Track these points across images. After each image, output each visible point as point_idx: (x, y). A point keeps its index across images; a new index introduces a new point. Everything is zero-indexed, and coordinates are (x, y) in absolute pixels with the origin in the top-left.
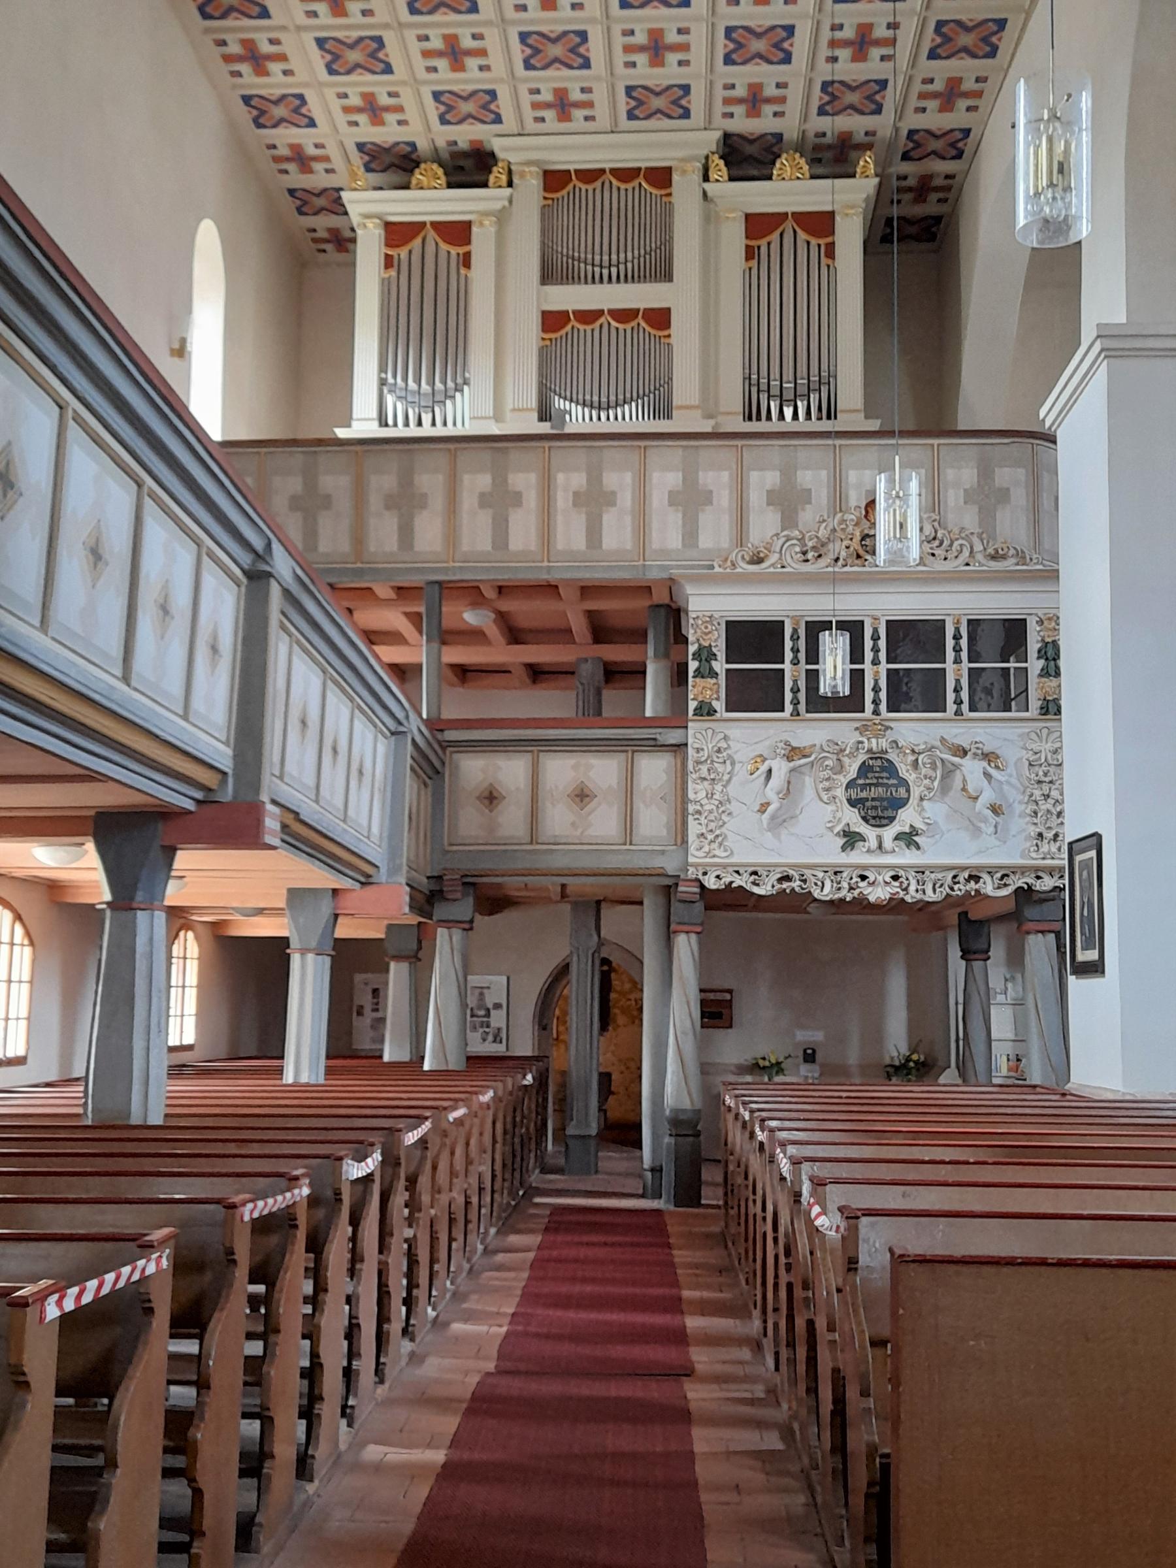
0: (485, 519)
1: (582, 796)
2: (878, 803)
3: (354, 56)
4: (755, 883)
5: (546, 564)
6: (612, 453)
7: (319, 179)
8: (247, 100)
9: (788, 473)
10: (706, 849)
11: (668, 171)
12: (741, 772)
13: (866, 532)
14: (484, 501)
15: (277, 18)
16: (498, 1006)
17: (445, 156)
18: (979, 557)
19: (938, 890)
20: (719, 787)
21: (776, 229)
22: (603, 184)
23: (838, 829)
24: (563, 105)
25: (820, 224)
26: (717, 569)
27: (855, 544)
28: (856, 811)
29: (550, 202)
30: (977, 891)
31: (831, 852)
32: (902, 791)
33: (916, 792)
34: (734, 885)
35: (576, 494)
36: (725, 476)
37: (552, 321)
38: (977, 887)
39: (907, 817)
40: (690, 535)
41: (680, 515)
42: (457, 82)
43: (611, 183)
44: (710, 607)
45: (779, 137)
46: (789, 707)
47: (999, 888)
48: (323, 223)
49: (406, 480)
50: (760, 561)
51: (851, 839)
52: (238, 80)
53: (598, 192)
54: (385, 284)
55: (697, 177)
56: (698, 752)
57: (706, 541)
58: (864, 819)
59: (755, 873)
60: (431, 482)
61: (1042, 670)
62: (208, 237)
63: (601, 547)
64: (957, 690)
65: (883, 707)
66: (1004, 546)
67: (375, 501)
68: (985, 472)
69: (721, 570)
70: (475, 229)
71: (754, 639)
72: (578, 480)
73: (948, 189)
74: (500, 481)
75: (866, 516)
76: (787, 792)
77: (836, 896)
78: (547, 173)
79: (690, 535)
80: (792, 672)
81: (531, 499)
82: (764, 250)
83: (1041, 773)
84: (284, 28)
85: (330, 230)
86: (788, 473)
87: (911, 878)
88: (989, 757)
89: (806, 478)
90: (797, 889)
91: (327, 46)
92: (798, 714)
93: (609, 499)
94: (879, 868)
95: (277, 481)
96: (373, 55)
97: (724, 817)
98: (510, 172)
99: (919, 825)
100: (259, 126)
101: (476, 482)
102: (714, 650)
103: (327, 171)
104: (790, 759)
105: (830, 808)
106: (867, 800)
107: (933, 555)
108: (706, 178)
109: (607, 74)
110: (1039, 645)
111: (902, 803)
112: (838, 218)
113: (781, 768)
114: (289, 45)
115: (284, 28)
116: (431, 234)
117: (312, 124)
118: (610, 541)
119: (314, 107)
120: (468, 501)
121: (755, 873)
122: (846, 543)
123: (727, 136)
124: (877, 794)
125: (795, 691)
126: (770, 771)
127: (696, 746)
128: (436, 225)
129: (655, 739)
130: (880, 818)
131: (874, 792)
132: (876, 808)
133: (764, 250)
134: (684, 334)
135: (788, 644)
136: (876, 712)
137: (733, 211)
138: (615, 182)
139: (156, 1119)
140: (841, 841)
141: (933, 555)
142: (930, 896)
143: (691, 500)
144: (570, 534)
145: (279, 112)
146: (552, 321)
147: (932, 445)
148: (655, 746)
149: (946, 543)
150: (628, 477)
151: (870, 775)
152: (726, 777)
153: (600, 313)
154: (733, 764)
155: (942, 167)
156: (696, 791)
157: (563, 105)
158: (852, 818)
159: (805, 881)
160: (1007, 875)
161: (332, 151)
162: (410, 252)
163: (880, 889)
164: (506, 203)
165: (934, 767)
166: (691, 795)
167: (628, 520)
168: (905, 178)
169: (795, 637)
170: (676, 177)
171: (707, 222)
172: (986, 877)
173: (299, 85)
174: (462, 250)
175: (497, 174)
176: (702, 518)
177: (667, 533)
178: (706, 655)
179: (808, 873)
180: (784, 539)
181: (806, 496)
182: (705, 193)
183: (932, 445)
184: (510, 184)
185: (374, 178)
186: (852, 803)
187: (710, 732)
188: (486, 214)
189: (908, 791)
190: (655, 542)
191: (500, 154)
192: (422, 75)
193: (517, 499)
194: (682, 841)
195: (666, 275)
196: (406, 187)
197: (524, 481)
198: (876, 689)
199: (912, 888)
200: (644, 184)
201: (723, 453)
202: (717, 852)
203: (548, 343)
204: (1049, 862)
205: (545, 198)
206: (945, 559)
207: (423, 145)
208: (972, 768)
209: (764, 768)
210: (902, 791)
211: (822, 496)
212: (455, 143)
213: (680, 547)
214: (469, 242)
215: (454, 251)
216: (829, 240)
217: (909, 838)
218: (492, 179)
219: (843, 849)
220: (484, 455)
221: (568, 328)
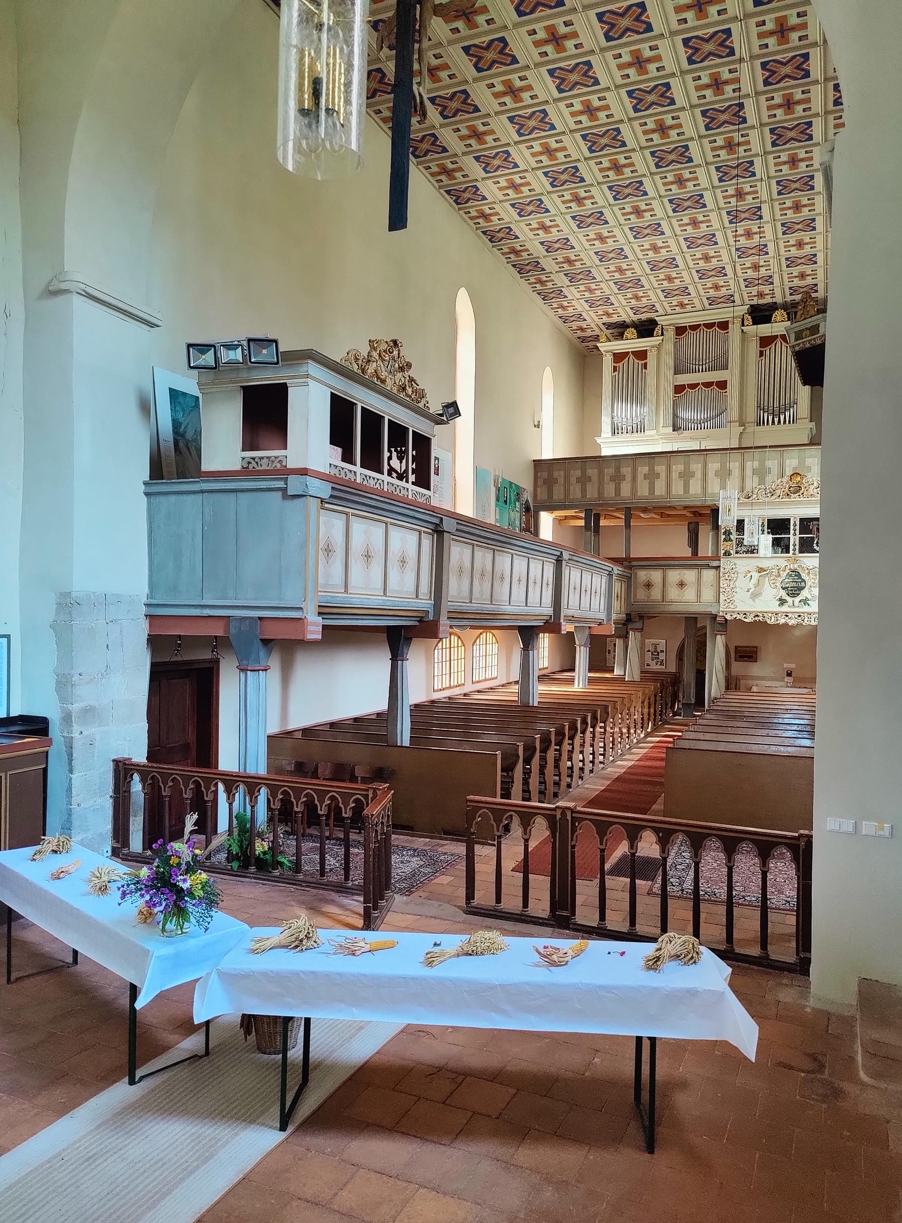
6: (694, 457)
7: (589, 333)
8: (560, 317)
9: (762, 462)
12: (741, 576)
14: (646, 477)
16: (662, 651)
24: (682, 305)
27: (787, 490)
31: (775, 606)
32: (803, 584)
33: (809, 584)
37: (679, 389)
45: (776, 303)
49: (618, 470)
54: (613, 378)
62: (548, 373)
67: (607, 478)
74: (652, 469)
78: (677, 328)
81: (663, 475)
82: (768, 352)
93: (692, 475)
99: (809, 597)
109: (699, 292)
113: (756, 575)
117: (585, 320)
120: (640, 477)
134: (733, 390)
139: (536, 704)
144: (678, 489)
146: (679, 389)
148: (708, 567)
153: (697, 385)
157: (682, 305)
158: (783, 594)
161: (593, 325)
175: (658, 330)
177: (714, 486)
178: (728, 533)
179: (765, 615)
186: (783, 589)
188: (653, 347)
190: (709, 491)
193: (658, 476)
197: (661, 469)
198: (795, 545)
201: (736, 455)
207: (628, 320)
209: (749, 575)
211: (775, 471)
220: (647, 460)
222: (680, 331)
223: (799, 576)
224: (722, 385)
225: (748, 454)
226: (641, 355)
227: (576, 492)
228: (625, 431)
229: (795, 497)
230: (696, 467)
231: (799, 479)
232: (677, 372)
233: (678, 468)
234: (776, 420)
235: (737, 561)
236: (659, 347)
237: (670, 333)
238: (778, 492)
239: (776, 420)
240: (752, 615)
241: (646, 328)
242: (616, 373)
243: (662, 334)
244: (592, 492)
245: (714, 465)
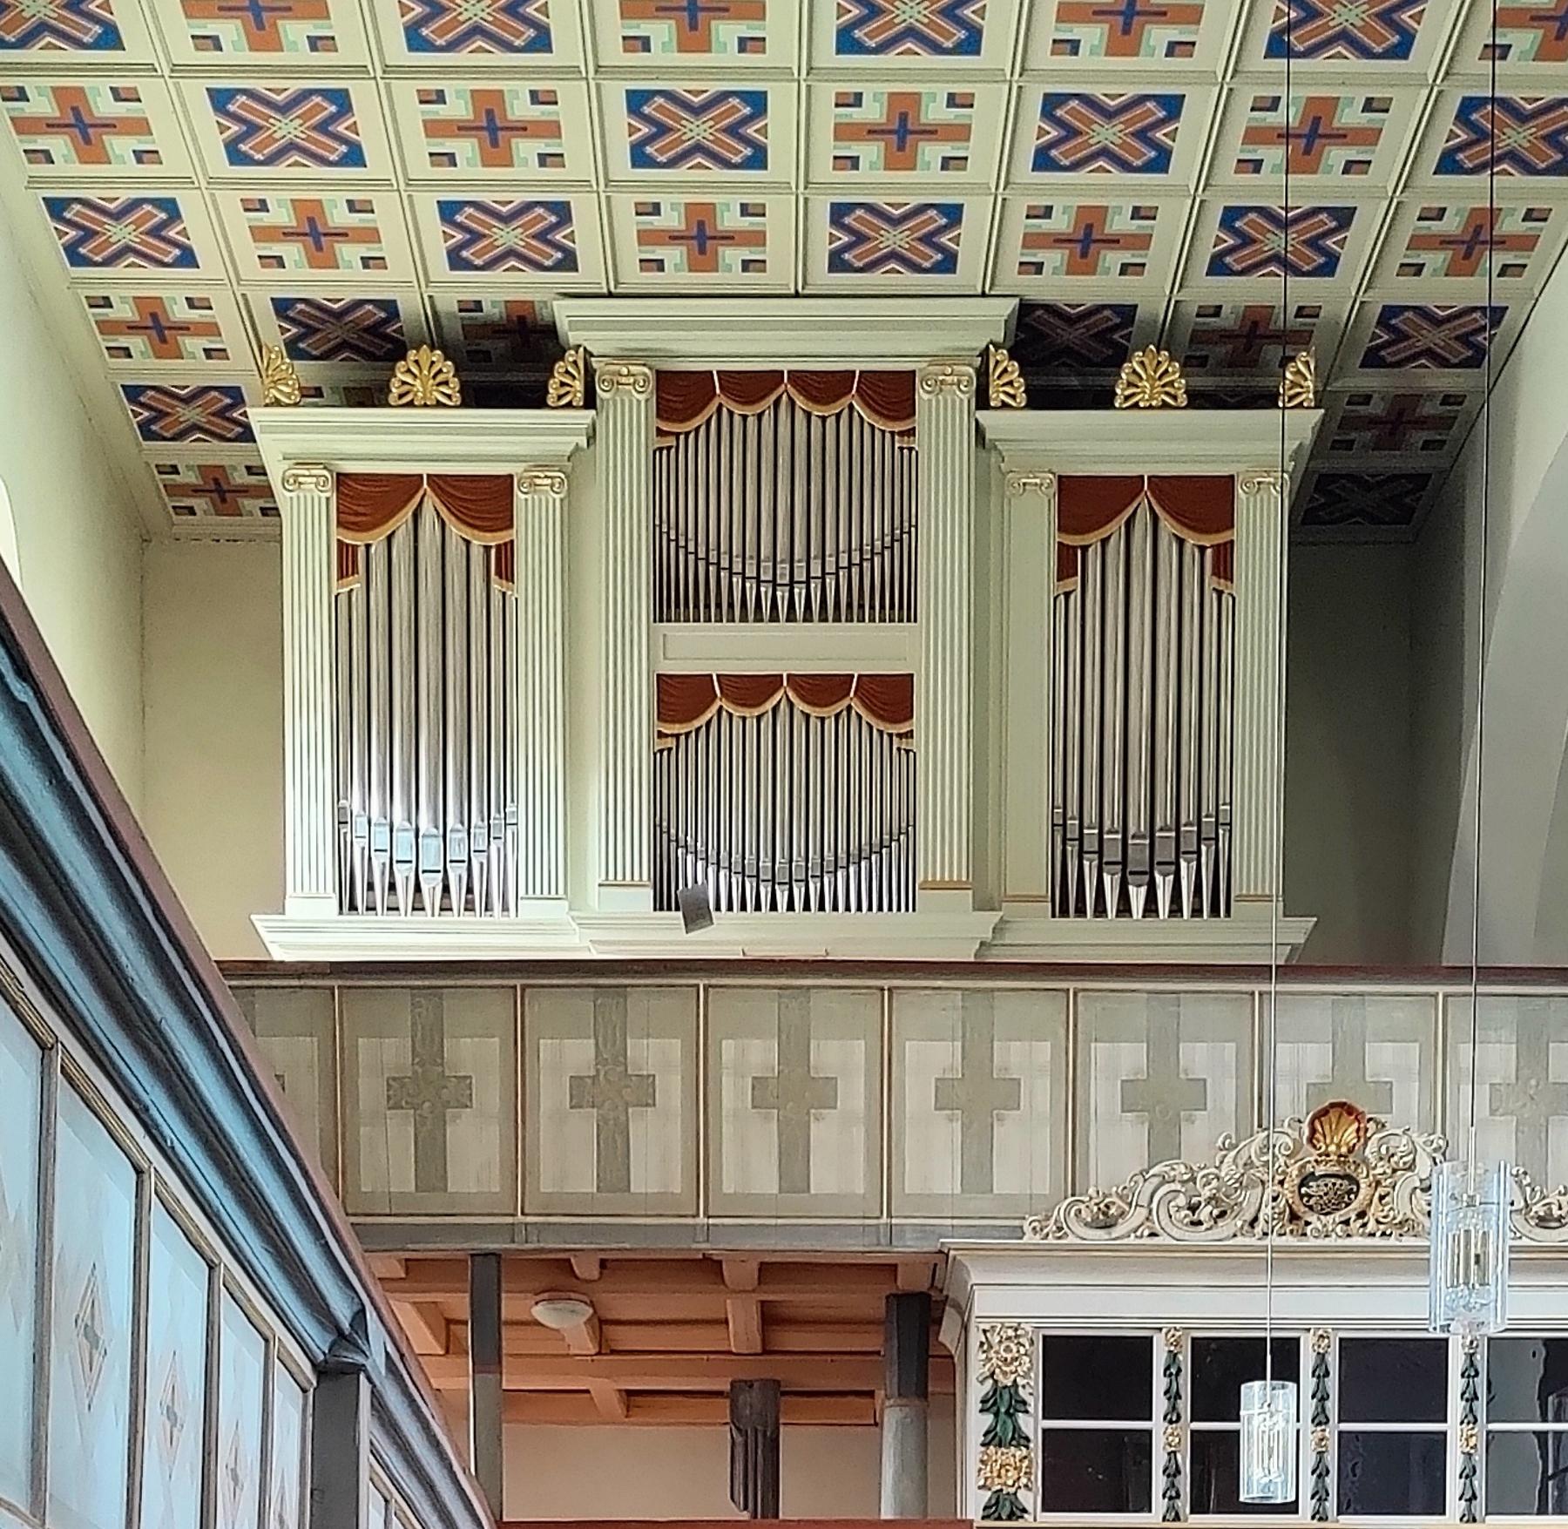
6: (828, 1001)
21: (1120, 512)
22: (777, 403)
25: (1203, 503)
29: (671, 441)
40: (977, 1165)
42: (489, 184)
43: (792, 403)
44: (1012, 1311)
46: (1159, 1503)
53: (767, 421)
57: (1006, 1180)
65: (1332, 1504)
69: (1037, 1239)
71: (1093, 1371)
72: (762, 1054)
73: (1446, 422)
78: (661, 376)
79: (977, 1165)
80: (1168, 1436)
81: (672, 1090)
92: (1177, 1518)
93: (824, 1093)
98: (589, 373)
112: (1240, 492)
118: (823, 1180)
133: (1094, 557)
135: (1159, 1383)
137: (1032, 472)
138: (800, 402)
143: (978, 1099)
150: (858, 1050)
167: (859, 1134)
168: (1366, 399)
169: (1172, 1370)
171: (979, 483)
182: (980, 431)
184: (590, 401)
185: (308, 372)
190: (911, 1181)
191: (573, 337)
197: (658, 1053)
205: (661, 433)
207: (411, 305)
212: (478, 306)
213: (958, 1190)
216: (1220, 538)
233: (747, 1054)
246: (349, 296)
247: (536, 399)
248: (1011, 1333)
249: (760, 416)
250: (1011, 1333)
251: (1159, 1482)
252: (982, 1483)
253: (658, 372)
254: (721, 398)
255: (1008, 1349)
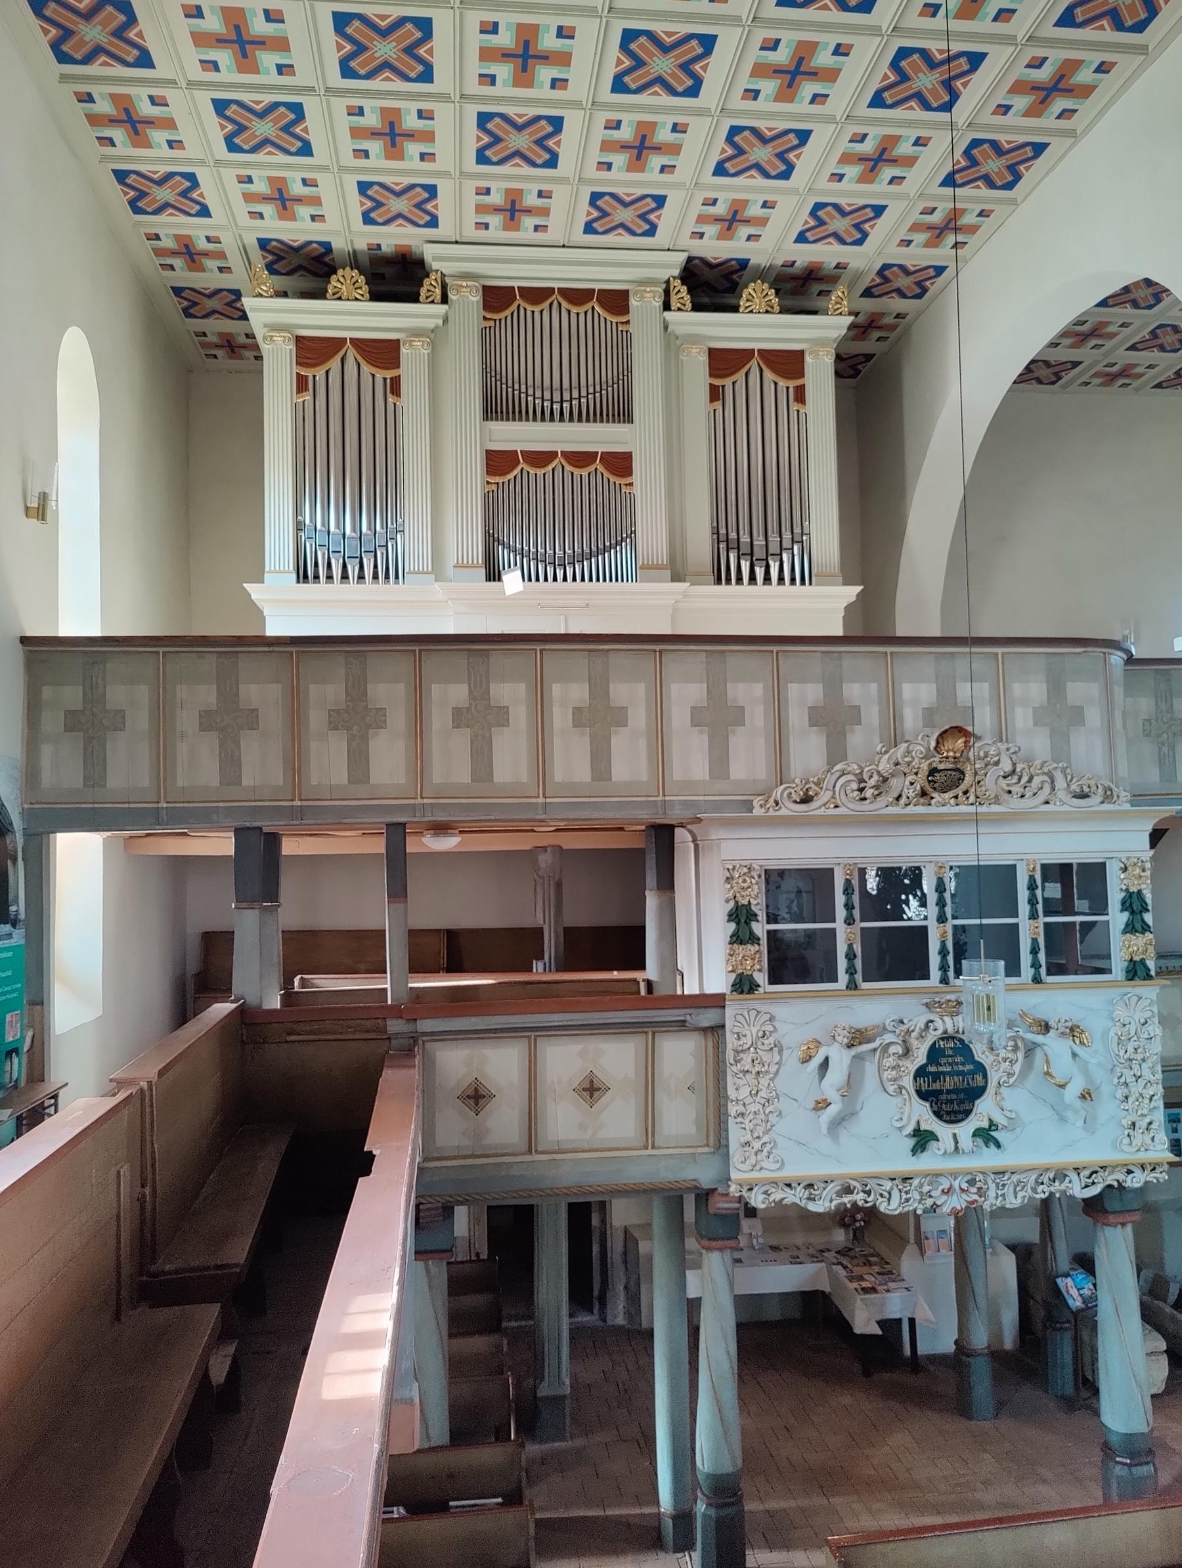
0: (461, 741)
1: (591, 1089)
2: (954, 1096)
3: (264, 128)
4: (811, 1199)
5: (541, 800)
6: (620, 659)
7: (209, 279)
8: (121, 176)
9: (833, 686)
10: (753, 1160)
11: (625, 294)
12: (791, 1059)
13: (934, 765)
14: (460, 717)
15: (163, 70)
17: (364, 261)
18: (1061, 794)
19: (1020, 1195)
20: (764, 1081)
22: (551, 305)
23: (910, 1129)
25: (788, 363)
26: (758, 811)
27: (921, 780)
28: (928, 1105)
30: (1064, 1192)
32: (979, 1078)
33: (994, 1077)
34: (784, 1202)
35: (577, 711)
36: (758, 689)
37: (498, 462)
38: (1063, 1187)
39: (984, 1109)
40: (720, 760)
41: (705, 737)
43: (560, 304)
45: (743, 264)
47: (1087, 1186)
48: (216, 326)
49: (357, 692)
50: (806, 800)
51: (922, 1139)
52: (109, 151)
55: (658, 303)
56: (739, 1038)
57: (738, 770)
58: (938, 1114)
59: (810, 1186)
60: (388, 691)
61: (1127, 925)
62: (75, 354)
63: (610, 779)
64: (1034, 951)
66: (1092, 783)
67: (316, 718)
68: (1056, 688)
70: (404, 350)
74: (479, 693)
75: (936, 748)
76: (851, 1086)
77: (906, 1209)
78: (487, 290)
79: (720, 760)
81: (520, 716)
83: (1131, 1050)
84: (172, 83)
85: (221, 335)
86: (833, 686)
87: (990, 1182)
88: (1073, 1031)
89: (854, 692)
90: (860, 1203)
91: (228, 113)
92: (856, 988)
93: (620, 717)
94: (955, 1175)
95: (182, 692)
96: (287, 129)
97: (773, 1119)
98: (444, 287)
99: (999, 1119)
100: (137, 210)
101: (449, 693)
102: (753, 908)
103: (221, 269)
104: (850, 1046)
105: (898, 1100)
106: (940, 1092)
107: (1010, 792)
108: (667, 306)
110: (1123, 894)
111: (980, 1092)
113: (840, 1059)
114: (178, 105)
115: (172, 83)
116: (352, 354)
117: (205, 212)
119: (208, 191)
120: (439, 719)
121: (810, 1186)
122: (910, 778)
123: (690, 259)
124: (950, 1085)
125: (851, 956)
126: (827, 1059)
127: (736, 1030)
128: (356, 342)
129: (684, 1021)
130: (956, 1112)
131: (949, 1083)
132: (951, 1101)
135: (840, 899)
136: (944, 980)
138: (565, 304)
140: (911, 1142)
141: (1010, 792)
142: (1013, 1202)
143: (718, 719)
144: (571, 763)
145: (164, 194)
146: (498, 462)
147: (996, 654)
149: (1025, 779)
151: (943, 1060)
152: (773, 1069)
153: (550, 456)
154: (780, 1052)
155: (897, 304)
156: (737, 1089)
158: (922, 1113)
159: (868, 1193)
160: (1096, 1172)
161: (228, 243)
162: (327, 372)
163: (955, 1197)
164: (440, 322)
165: (1016, 1048)
166: (731, 1092)
167: (642, 744)
170: (633, 302)
172: (1073, 1175)
173: (189, 162)
174: (389, 374)
175: (430, 285)
176: (732, 740)
177: (691, 760)
179: (872, 1184)
180: (838, 774)
181: (855, 715)
183: (996, 654)
186: (923, 1095)
187: (753, 1013)
188: (417, 333)
189: (985, 1077)
190: (677, 773)
192: (348, 159)
193: (502, 716)
194: (721, 1146)
195: (624, 414)
196: (320, 294)
197: (511, 693)
199: (992, 1193)
200: (597, 308)
202: (765, 1164)
203: (494, 487)
204: (1143, 1156)
206: (1022, 796)
208: (1056, 1047)
210: (979, 1078)
211: (872, 715)
212: (379, 246)
213: (707, 777)
214: (397, 365)
215: (380, 375)
217: (986, 1135)
218: (423, 292)
219: (914, 1151)
220: (459, 660)
221: (517, 471)
222: (496, 298)
223: (964, 1050)
224: (620, 464)
225: (790, 661)
226: (383, 353)
227: (198, 767)
228: (337, 571)
229: (942, 803)
230: (629, 693)
231: (960, 742)
232: (493, 409)
234: (760, 572)
235: (781, 1011)
236: (434, 337)
237: (469, 299)
238: (896, 784)
239: (760, 572)
240: (833, 1188)
241: (397, 277)
242: (308, 397)
243: (445, 300)
244: (261, 769)
245: (686, 692)
246: (302, 238)
247: (413, 298)
248: (745, 870)
249: (542, 312)
250: (745, 870)
251: (842, 964)
252: (730, 968)
253: (484, 287)
254: (519, 300)
255: (745, 881)
